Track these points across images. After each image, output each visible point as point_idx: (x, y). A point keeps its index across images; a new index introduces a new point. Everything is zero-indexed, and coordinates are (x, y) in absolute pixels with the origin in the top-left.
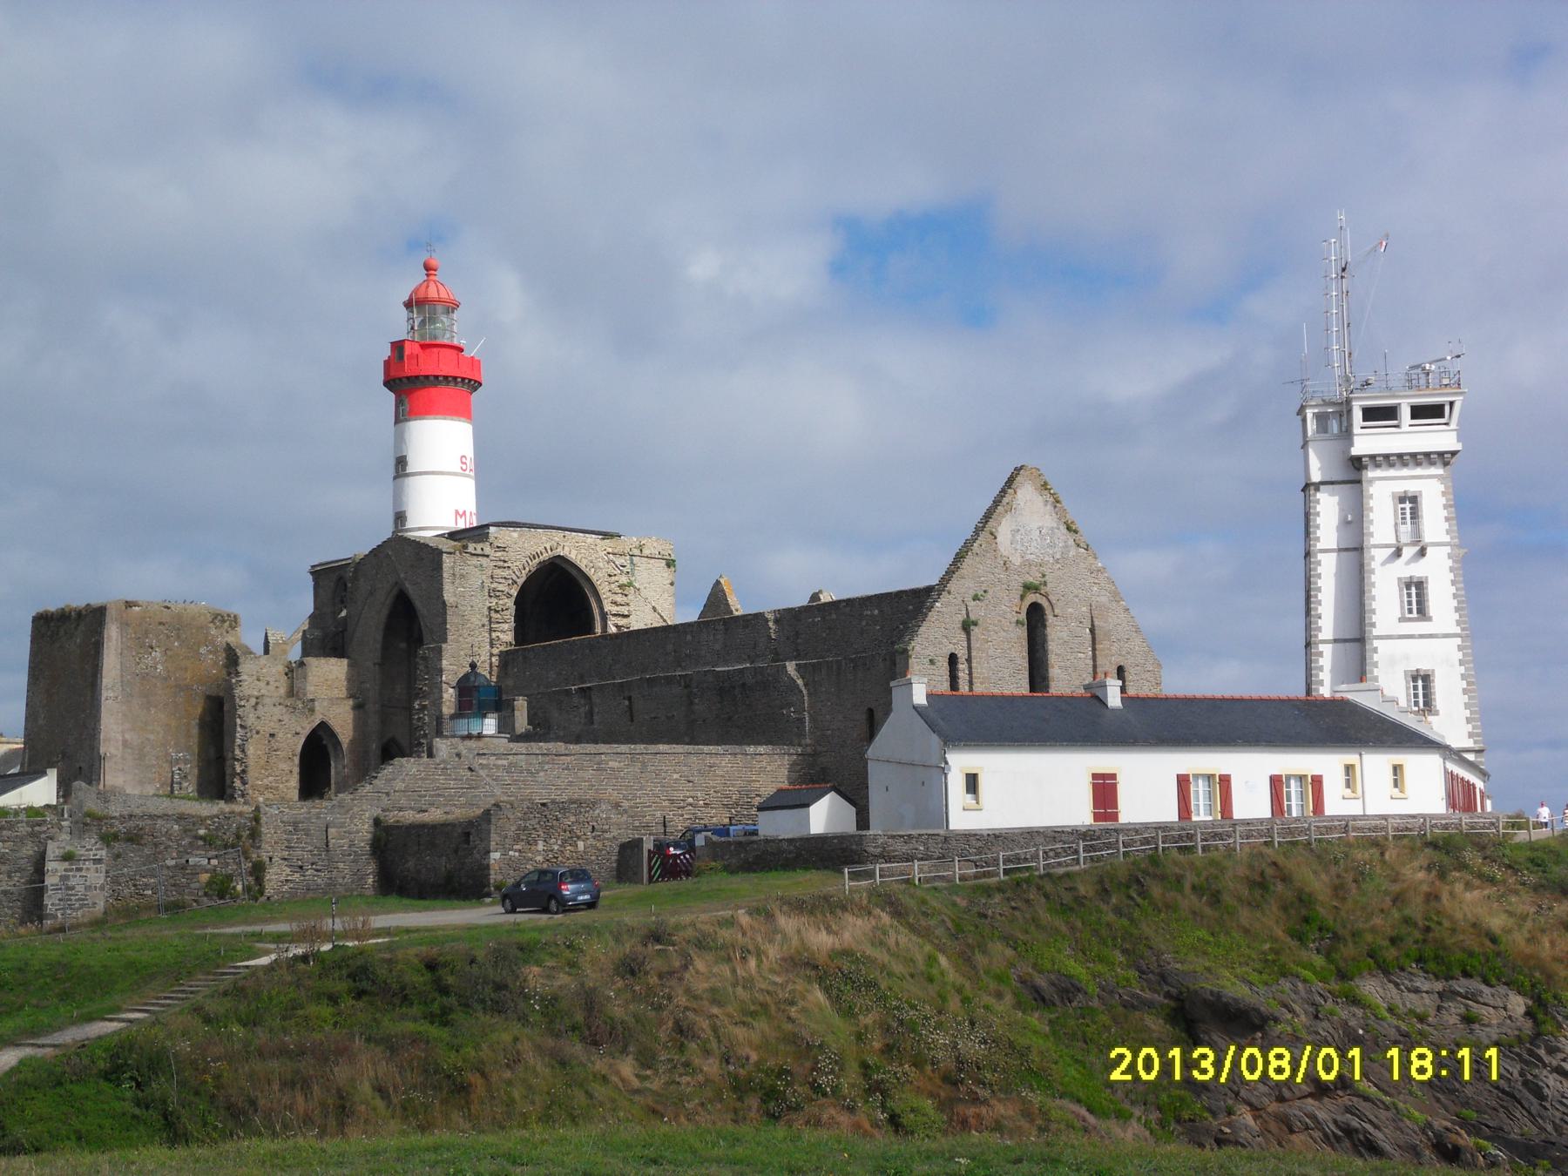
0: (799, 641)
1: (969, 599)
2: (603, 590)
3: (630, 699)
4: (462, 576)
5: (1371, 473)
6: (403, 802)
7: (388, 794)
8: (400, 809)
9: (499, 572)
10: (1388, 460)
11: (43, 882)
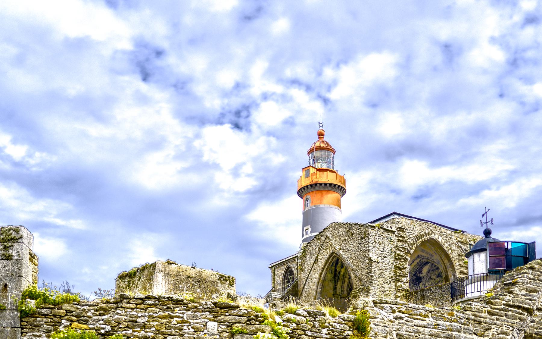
2: (456, 263)
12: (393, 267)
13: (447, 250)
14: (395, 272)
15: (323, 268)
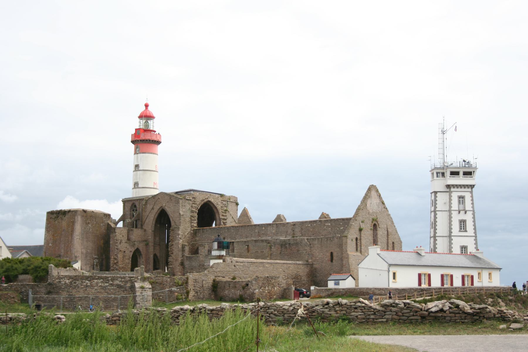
0: (303, 231)
1: (361, 222)
2: (220, 211)
3: (248, 246)
4: (184, 206)
6: (220, 275)
7: (216, 272)
8: (219, 277)
9: (193, 205)
10: (457, 186)
11: (152, 294)
12: (190, 217)
13: (215, 205)
14: (191, 218)
15: (156, 213)
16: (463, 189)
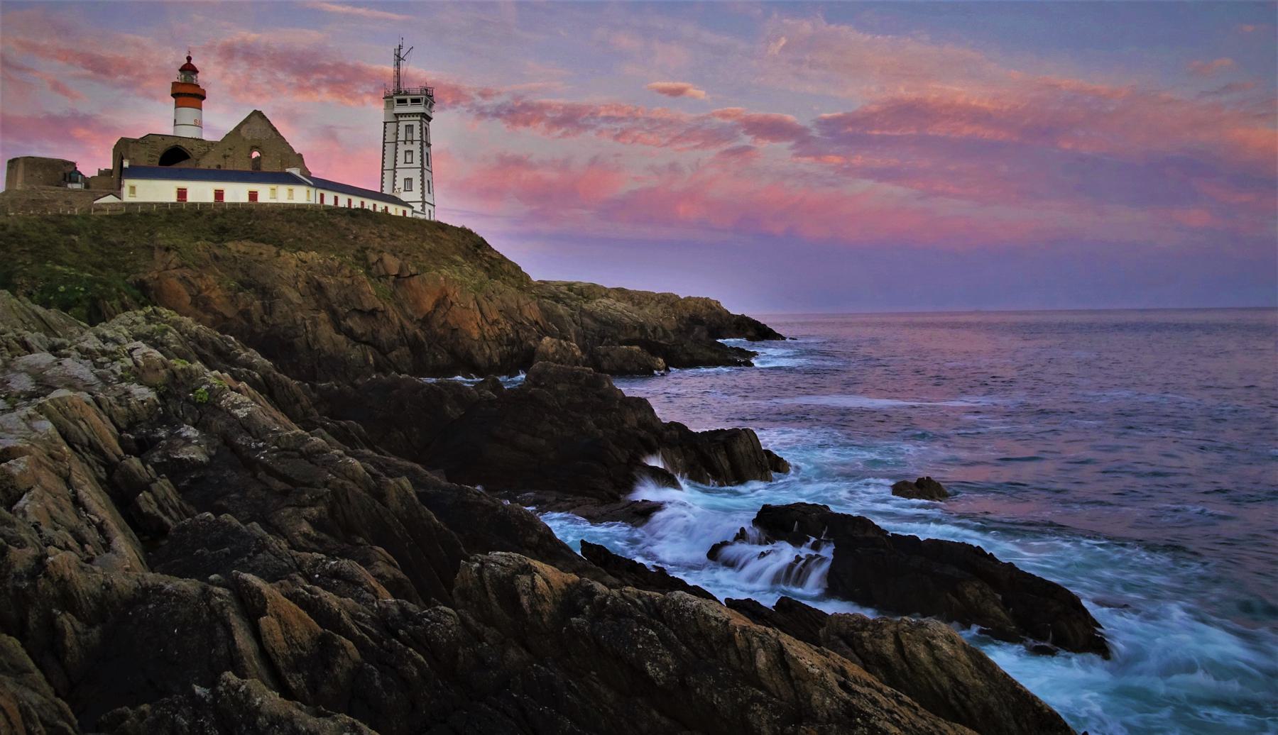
5: (400, 119)
16: (411, 118)
